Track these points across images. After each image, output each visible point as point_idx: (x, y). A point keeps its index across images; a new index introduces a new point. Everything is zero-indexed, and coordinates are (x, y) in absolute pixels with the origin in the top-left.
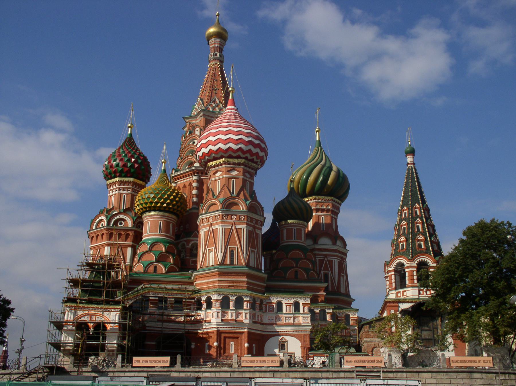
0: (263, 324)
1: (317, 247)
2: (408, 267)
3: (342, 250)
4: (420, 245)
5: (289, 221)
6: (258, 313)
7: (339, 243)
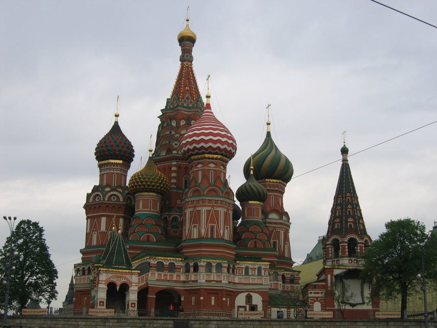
0: (235, 283)
1: (268, 220)
2: (341, 243)
3: (286, 223)
4: (350, 225)
5: (250, 202)
6: (232, 276)
7: (284, 218)
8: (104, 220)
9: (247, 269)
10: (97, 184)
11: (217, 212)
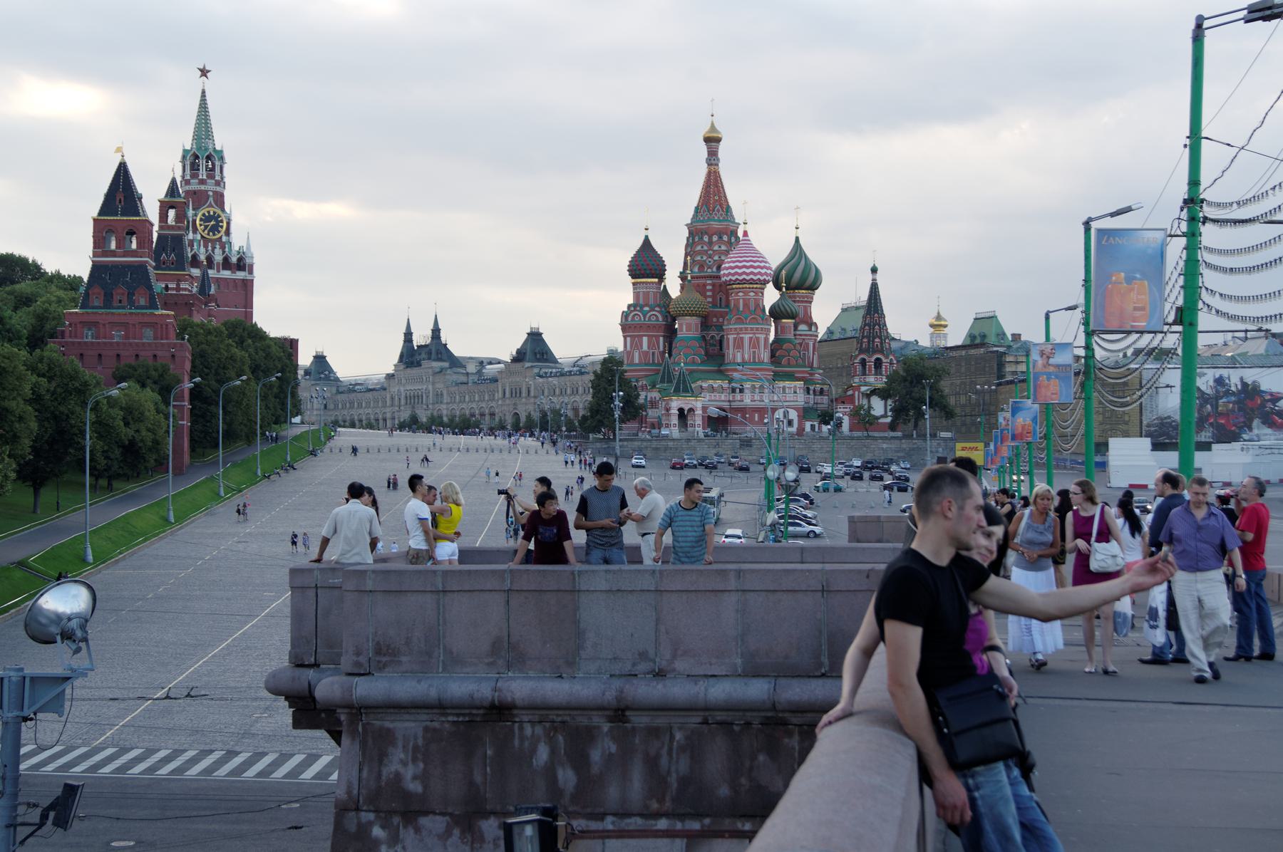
8: (645, 339)
9: (784, 388)
10: (631, 302)
11: (758, 339)
